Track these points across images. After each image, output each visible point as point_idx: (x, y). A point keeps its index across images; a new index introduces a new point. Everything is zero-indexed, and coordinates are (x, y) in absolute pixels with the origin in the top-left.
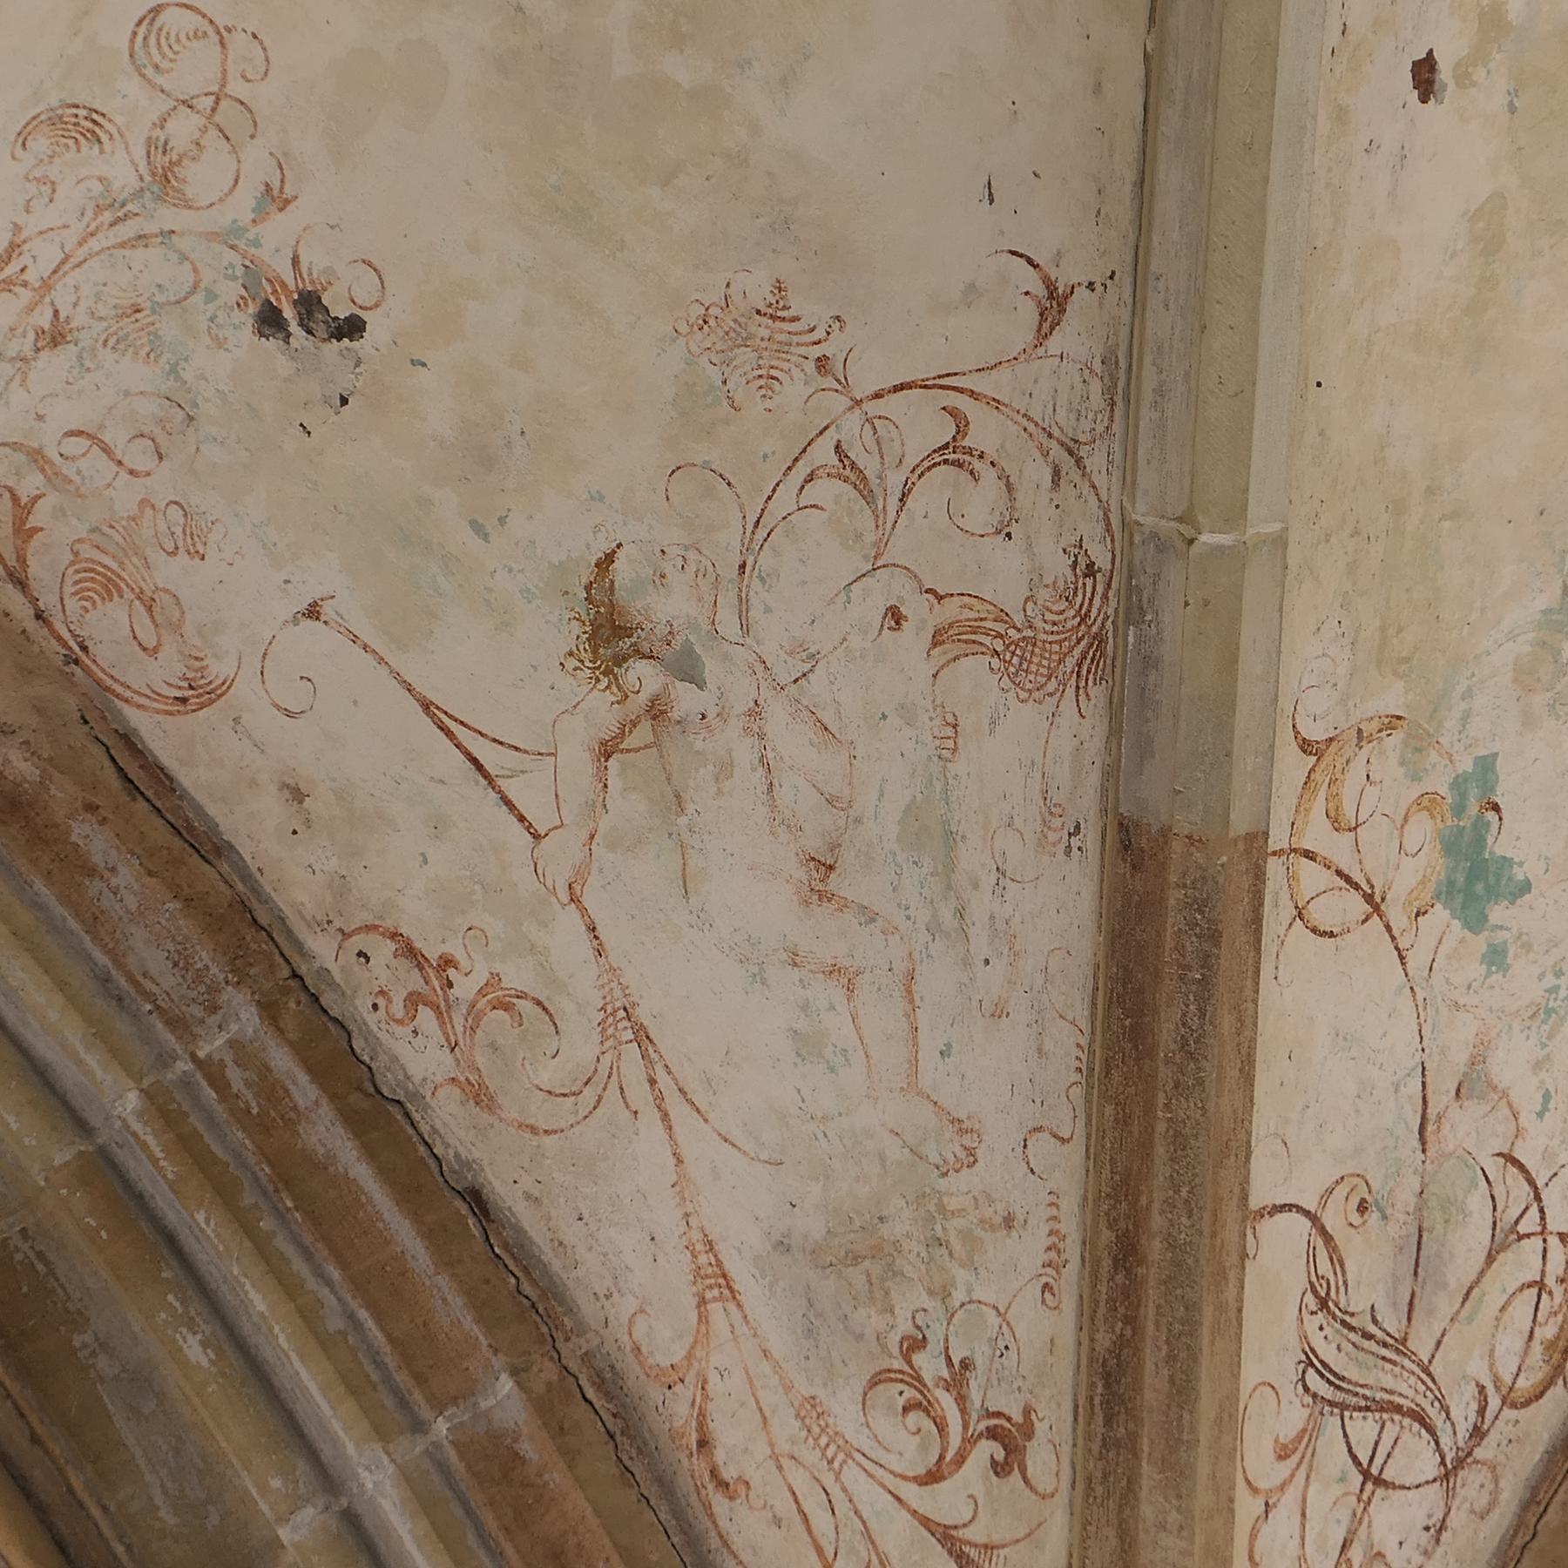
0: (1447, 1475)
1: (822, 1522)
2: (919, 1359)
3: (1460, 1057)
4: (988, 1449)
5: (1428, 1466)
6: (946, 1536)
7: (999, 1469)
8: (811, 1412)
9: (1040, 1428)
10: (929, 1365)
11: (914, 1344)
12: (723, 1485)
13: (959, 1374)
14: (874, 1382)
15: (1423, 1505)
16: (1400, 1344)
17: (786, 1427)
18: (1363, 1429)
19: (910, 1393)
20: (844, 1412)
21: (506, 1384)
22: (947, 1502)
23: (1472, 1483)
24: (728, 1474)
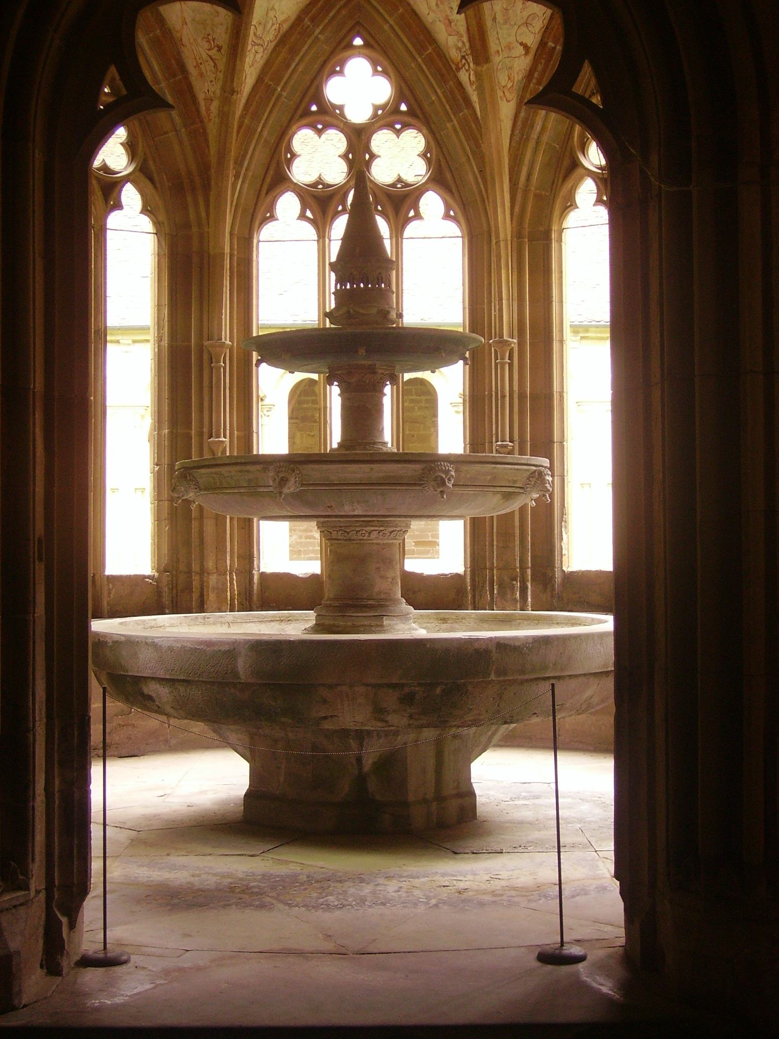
0: (264, 51)
1: (195, 52)
2: (209, 37)
3: (271, 6)
4: (216, 48)
5: (262, 50)
6: (210, 56)
7: (218, 51)
8: (195, 40)
9: (223, 48)
10: (210, 37)
11: (209, 35)
12: (183, 45)
13: (214, 40)
14: (204, 38)
15: (261, 55)
16: (261, 38)
17: (192, 40)
18: (256, 47)
19: (207, 40)
20: (199, 40)
21: (158, 31)
22: (211, 53)
23: (266, 52)
24: (184, 44)
